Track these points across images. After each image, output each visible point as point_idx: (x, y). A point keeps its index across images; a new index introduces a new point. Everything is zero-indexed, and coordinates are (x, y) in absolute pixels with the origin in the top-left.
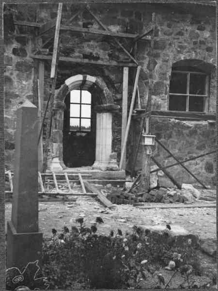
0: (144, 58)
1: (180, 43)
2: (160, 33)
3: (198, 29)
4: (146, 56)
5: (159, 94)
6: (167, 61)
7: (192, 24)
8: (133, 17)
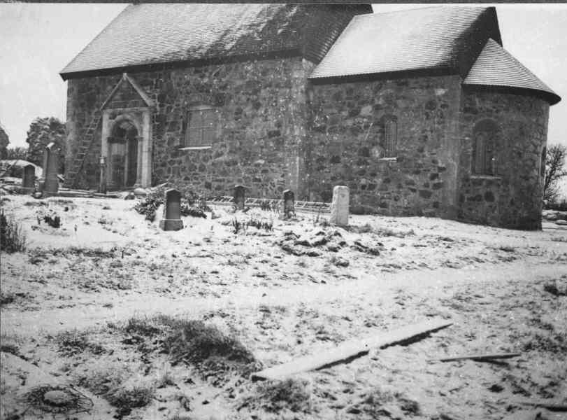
5: (174, 130)
6: (179, 105)
7: (196, 72)
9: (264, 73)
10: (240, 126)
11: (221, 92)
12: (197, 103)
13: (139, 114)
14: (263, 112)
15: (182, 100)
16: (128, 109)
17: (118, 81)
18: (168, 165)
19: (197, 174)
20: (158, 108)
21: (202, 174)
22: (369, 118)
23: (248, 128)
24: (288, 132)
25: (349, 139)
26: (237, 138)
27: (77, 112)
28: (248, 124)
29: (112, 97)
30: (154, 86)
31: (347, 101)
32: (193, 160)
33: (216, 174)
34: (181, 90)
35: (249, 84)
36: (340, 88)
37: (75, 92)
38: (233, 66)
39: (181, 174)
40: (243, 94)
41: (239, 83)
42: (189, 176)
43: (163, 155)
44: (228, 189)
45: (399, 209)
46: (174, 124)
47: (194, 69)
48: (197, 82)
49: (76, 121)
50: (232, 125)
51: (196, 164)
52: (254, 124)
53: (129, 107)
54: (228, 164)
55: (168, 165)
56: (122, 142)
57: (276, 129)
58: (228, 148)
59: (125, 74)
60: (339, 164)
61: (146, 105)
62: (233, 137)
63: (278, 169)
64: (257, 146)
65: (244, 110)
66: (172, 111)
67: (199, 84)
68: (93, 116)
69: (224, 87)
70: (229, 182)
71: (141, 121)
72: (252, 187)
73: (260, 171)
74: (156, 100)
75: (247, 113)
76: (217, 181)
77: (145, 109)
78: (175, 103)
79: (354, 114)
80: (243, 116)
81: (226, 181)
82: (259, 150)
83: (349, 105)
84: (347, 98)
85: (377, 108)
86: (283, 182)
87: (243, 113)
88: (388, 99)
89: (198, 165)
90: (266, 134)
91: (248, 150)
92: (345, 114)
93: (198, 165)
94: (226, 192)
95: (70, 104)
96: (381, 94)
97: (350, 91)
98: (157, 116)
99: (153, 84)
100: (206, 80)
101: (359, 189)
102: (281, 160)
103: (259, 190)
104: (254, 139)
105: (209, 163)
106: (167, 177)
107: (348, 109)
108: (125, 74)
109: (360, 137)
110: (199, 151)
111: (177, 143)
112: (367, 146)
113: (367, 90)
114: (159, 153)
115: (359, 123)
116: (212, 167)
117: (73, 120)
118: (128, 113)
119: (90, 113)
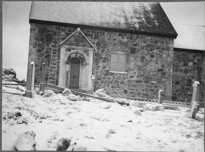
0: (100, 49)
1: (114, 43)
2: (106, 39)
3: (122, 38)
4: (101, 48)
5: (106, 62)
6: (109, 50)
7: (119, 35)
8: (96, 34)
9: (156, 42)
10: (144, 64)
11: (134, 47)
12: (118, 50)
13: (86, 52)
14: (155, 60)
15: (111, 48)
16: (79, 47)
17: (74, 31)
18: (102, 80)
19: (119, 85)
20: (96, 49)
21: (122, 86)
22: (191, 67)
23: (148, 66)
24: (167, 70)
25: (184, 75)
26: (142, 70)
27: (38, 43)
28: (148, 64)
29: (69, 39)
30: (93, 38)
31: (183, 59)
32: (117, 78)
33: (130, 86)
34: (111, 42)
35: (148, 46)
36: (180, 53)
37: (37, 31)
38: (140, 36)
39: (110, 85)
40: (146, 50)
41: (143, 44)
42: (114, 86)
43: (99, 74)
44: (137, 94)
45: (202, 105)
46: (105, 59)
47: (118, 33)
48: (120, 40)
49: (37, 48)
50: (140, 64)
51: (118, 80)
52: (150, 64)
53: (80, 46)
54: (137, 82)
55: (102, 80)
56: (69, 64)
57: (162, 68)
58: (137, 74)
59: (79, 29)
60: (179, 85)
61: (92, 47)
62: (140, 69)
63: (162, 86)
64: (152, 75)
65: (146, 57)
66: (105, 52)
67: (121, 41)
68: (50, 46)
69: (136, 45)
70: (137, 90)
71: (88, 55)
72: (149, 94)
73: (154, 86)
74: (95, 45)
75: (147, 59)
76: (131, 89)
77: (91, 49)
78: (107, 48)
79: (186, 65)
80: (145, 60)
81: (135, 90)
82: (153, 77)
83: (184, 61)
84: (182, 58)
85: (195, 64)
86: (165, 92)
87: (145, 59)
88: (199, 60)
89: (120, 81)
90: (157, 70)
91: (148, 76)
92: (182, 64)
93: (120, 81)
94: (135, 95)
95: (33, 38)
96: (196, 58)
97: (184, 55)
98: (95, 53)
99: (93, 36)
100: (125, 40)
101: (187, 96)
102: (163, 82)
103: (153, 95)
104: (151, 71)
105: (126, 80)
106: (101, 85)
107: (183, 62)
108: (79, 29)
109: (188, 74)
110: (121, 74)
111: (107, 69)
112: (191, 79)
113: (191, 56)
114: (96, 73)
115: (187, 68)
116: (128, 83)
117: (35, 47)
118: (80, 50)
119: (48, 45)
